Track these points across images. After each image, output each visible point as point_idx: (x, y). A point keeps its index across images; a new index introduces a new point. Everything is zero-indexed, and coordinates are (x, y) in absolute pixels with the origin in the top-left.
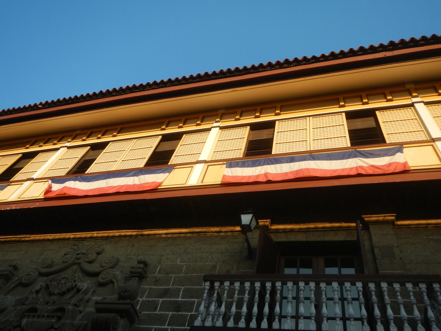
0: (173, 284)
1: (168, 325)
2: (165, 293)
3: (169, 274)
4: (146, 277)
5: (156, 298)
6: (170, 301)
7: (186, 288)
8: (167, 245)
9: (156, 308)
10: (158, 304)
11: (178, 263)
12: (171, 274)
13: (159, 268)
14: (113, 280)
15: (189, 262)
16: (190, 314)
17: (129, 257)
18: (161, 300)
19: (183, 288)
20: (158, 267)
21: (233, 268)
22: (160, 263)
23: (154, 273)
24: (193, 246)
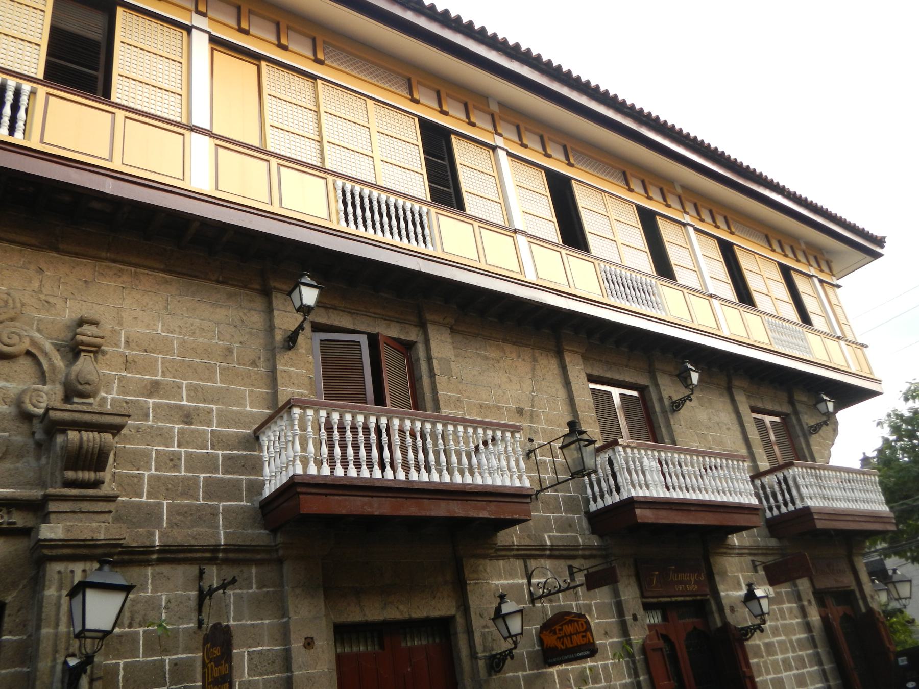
0: (163, 372)
1: (179, 446)
2: (154, 389)
3: (150, 352)
4: (104, 353)
5: (138, 396)
6: (168, 405)
7: (191, 383)
8: (123, 287)
9: (147, 416)
10: (149, 408)
11: (159, 332)
12: (153, 353)
13: (123, 336)
14: (34, 351)
15: (180, 333)
16: (210, 429)
17: (43, 297)
18: (151, 401)
19: (185, 382)
20: (120, 333)
21: (260, 358)
22: (120, 323)
23: (117, 345)
24: (179, 301)
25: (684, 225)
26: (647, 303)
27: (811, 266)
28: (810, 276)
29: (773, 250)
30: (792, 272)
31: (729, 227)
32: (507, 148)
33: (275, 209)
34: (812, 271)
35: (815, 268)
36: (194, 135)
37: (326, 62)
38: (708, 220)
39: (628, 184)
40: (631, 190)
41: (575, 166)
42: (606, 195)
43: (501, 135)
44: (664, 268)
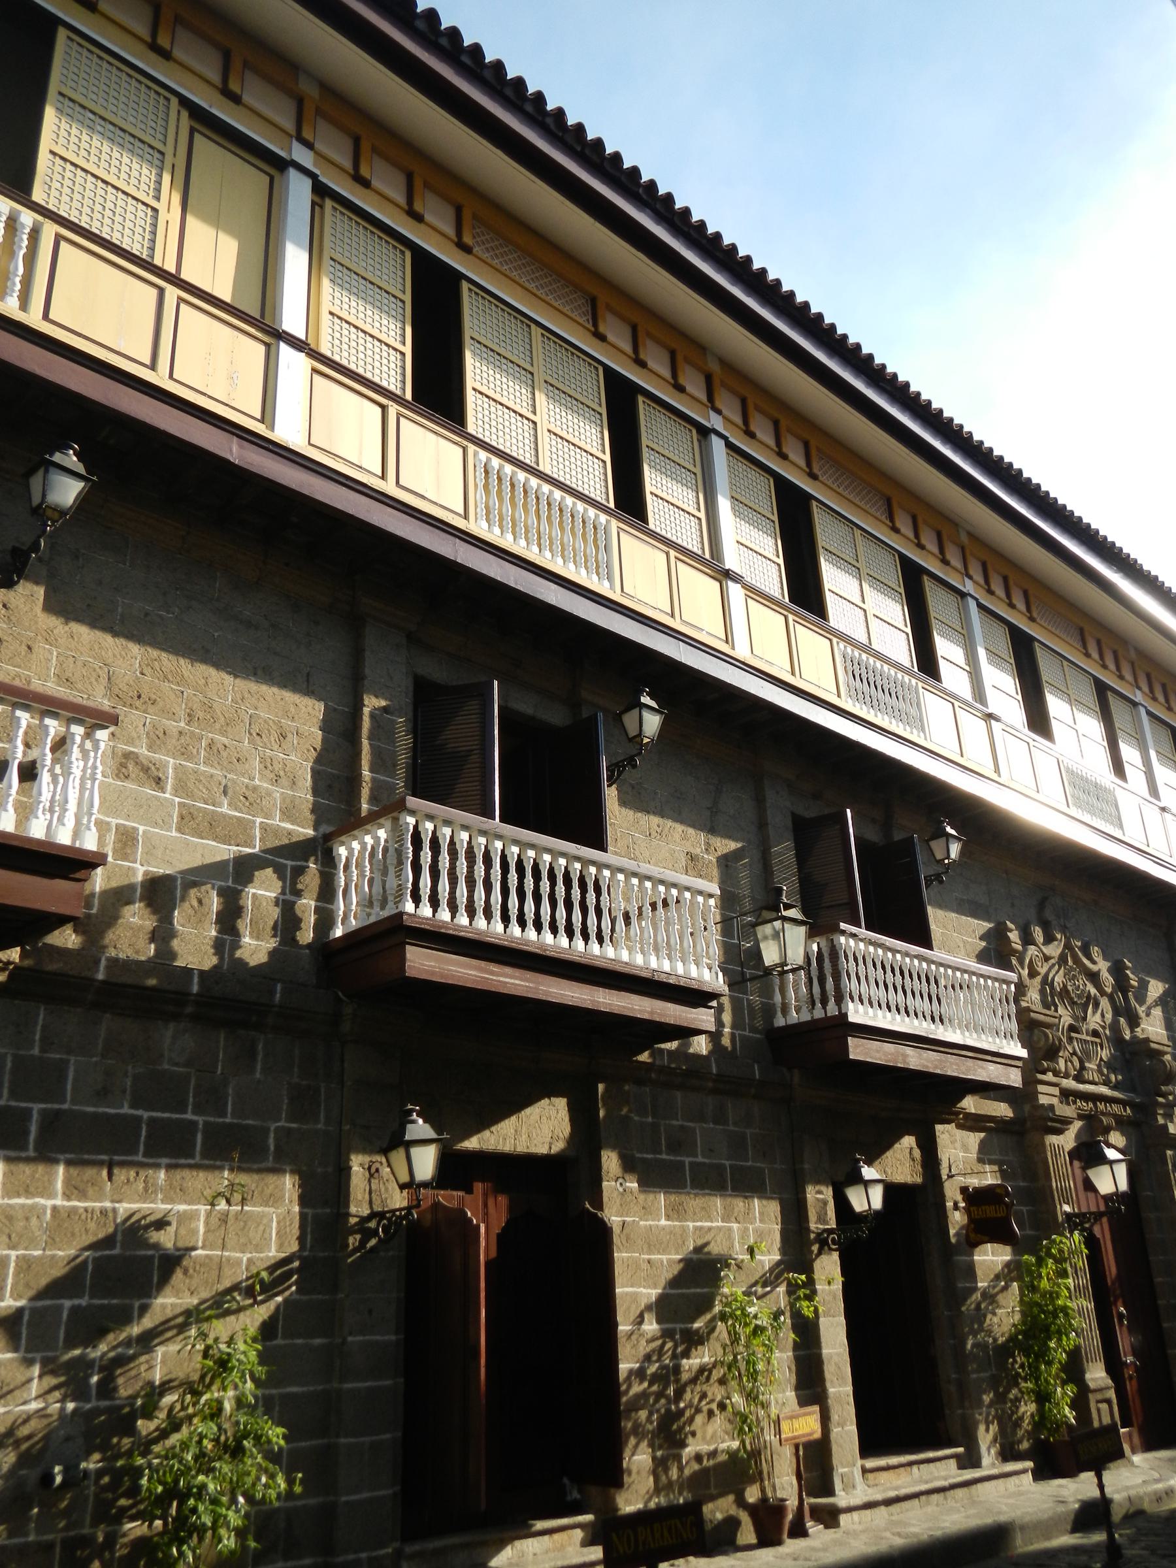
25: (963, 595)
26: (901, 716)
27: (1139, 688)
28: (1135, 704)
29: (1088, 655)
30: (1109, 694)
31: (1029, 609)
32: (727, 434)
33: (389, 488)
34: (1138, 697)
35: (1143, 692)
36: (284, 348)
37: (475, 250)
38: (1000, 592)
39: (891, 518)
40: (896, 530)
41: (820, 477)
42: (859, 532)
43: (719, 412)
44: (927, 663)
